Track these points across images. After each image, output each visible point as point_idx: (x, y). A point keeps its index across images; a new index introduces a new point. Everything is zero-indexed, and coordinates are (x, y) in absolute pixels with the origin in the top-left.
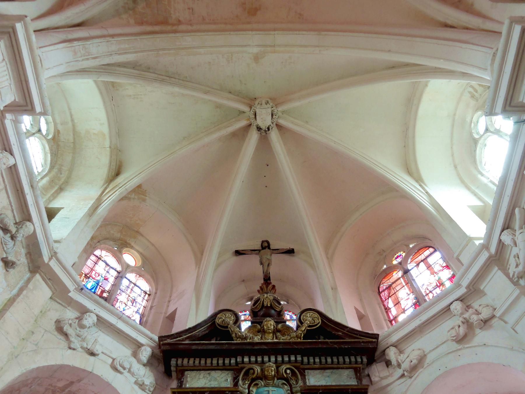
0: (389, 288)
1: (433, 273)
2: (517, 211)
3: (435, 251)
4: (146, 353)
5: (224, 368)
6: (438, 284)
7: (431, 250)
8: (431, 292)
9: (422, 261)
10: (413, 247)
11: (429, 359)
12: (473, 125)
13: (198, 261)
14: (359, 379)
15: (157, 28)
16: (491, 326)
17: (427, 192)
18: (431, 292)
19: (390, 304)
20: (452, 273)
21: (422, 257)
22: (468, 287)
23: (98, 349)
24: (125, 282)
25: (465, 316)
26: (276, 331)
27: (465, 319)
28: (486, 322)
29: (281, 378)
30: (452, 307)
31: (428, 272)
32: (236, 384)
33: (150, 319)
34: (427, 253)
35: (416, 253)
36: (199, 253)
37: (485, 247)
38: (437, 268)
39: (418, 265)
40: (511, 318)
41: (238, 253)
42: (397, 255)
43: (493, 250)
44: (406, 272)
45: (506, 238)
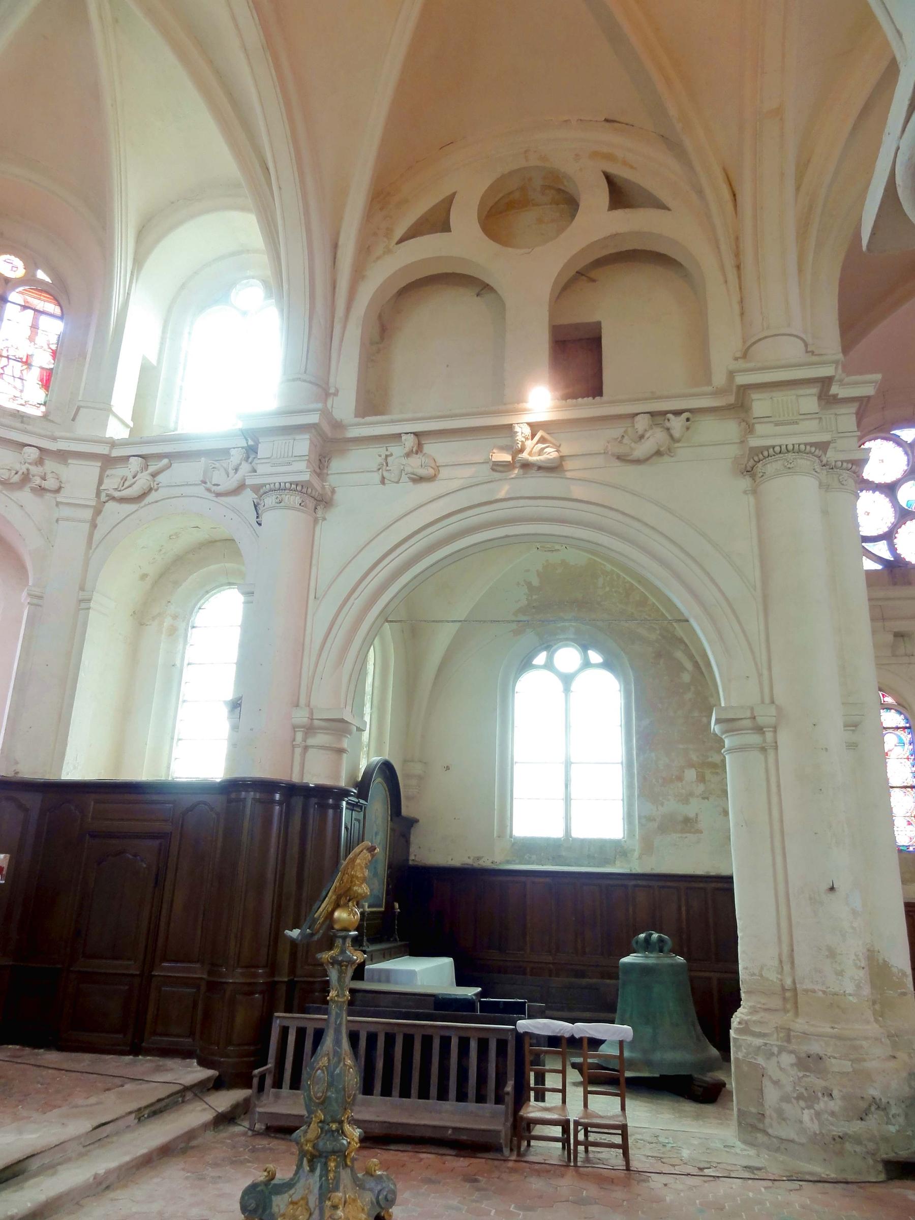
1: (31, 339)
2: (165, 461)
3: (61, 318)
6: (24, 360)
7: (57, 311)
8: (8, 357)
9: (35, 310)
10: (42, 282)
12: (245, 281)
16: (41, 496)
17: (129, 294)
18: (8, 357)
20: (52, 366)
21: (40, 304)
22: (60, 451)
25: (30, 467)
27: (28, 470)
28: (41, 490)
30: (26, 449)
31: (28, 332)
34: (51, 307)
35: (36, 289)
37: (113, 444)
38: (41, 339)
39: (25, 307)
40: (65, 512)
42: (12, 257)
43: (115, 453)
45: (135, 464)
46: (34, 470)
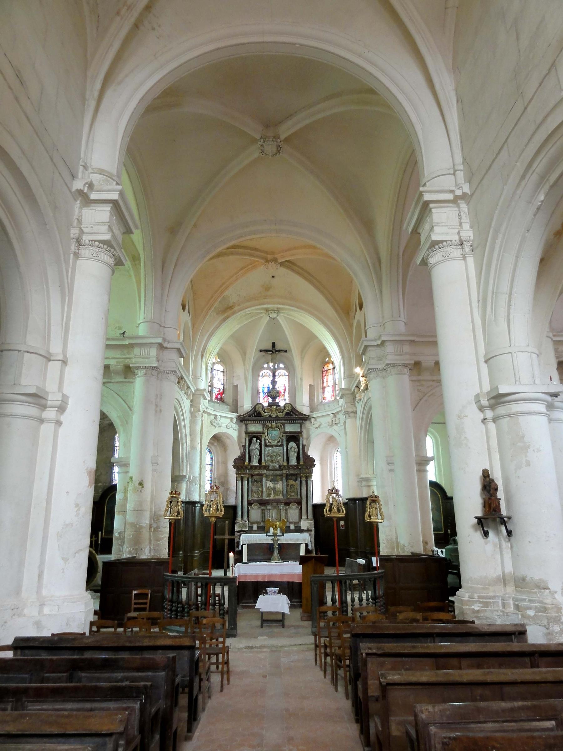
0: (327, 371)
4: (235, 420)
5: (259, 424)
11: (322, 426)
13: (244, 360)
14: (301, 427)
15: (226, 315)
19: (325, 380)
23: (222, 425)
24: (214, 372)
26: (276, 410)
29: (277, 428)
32: (263, 430)
33: (227, 387)
36: (244, 354)
41: (261, 351)
44: (334, 368)
46: (334, 419)
